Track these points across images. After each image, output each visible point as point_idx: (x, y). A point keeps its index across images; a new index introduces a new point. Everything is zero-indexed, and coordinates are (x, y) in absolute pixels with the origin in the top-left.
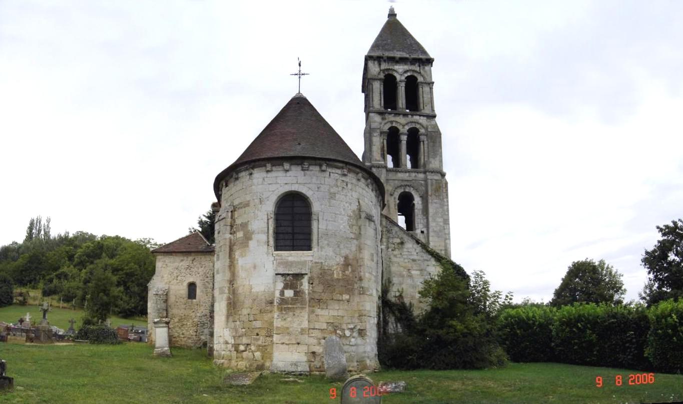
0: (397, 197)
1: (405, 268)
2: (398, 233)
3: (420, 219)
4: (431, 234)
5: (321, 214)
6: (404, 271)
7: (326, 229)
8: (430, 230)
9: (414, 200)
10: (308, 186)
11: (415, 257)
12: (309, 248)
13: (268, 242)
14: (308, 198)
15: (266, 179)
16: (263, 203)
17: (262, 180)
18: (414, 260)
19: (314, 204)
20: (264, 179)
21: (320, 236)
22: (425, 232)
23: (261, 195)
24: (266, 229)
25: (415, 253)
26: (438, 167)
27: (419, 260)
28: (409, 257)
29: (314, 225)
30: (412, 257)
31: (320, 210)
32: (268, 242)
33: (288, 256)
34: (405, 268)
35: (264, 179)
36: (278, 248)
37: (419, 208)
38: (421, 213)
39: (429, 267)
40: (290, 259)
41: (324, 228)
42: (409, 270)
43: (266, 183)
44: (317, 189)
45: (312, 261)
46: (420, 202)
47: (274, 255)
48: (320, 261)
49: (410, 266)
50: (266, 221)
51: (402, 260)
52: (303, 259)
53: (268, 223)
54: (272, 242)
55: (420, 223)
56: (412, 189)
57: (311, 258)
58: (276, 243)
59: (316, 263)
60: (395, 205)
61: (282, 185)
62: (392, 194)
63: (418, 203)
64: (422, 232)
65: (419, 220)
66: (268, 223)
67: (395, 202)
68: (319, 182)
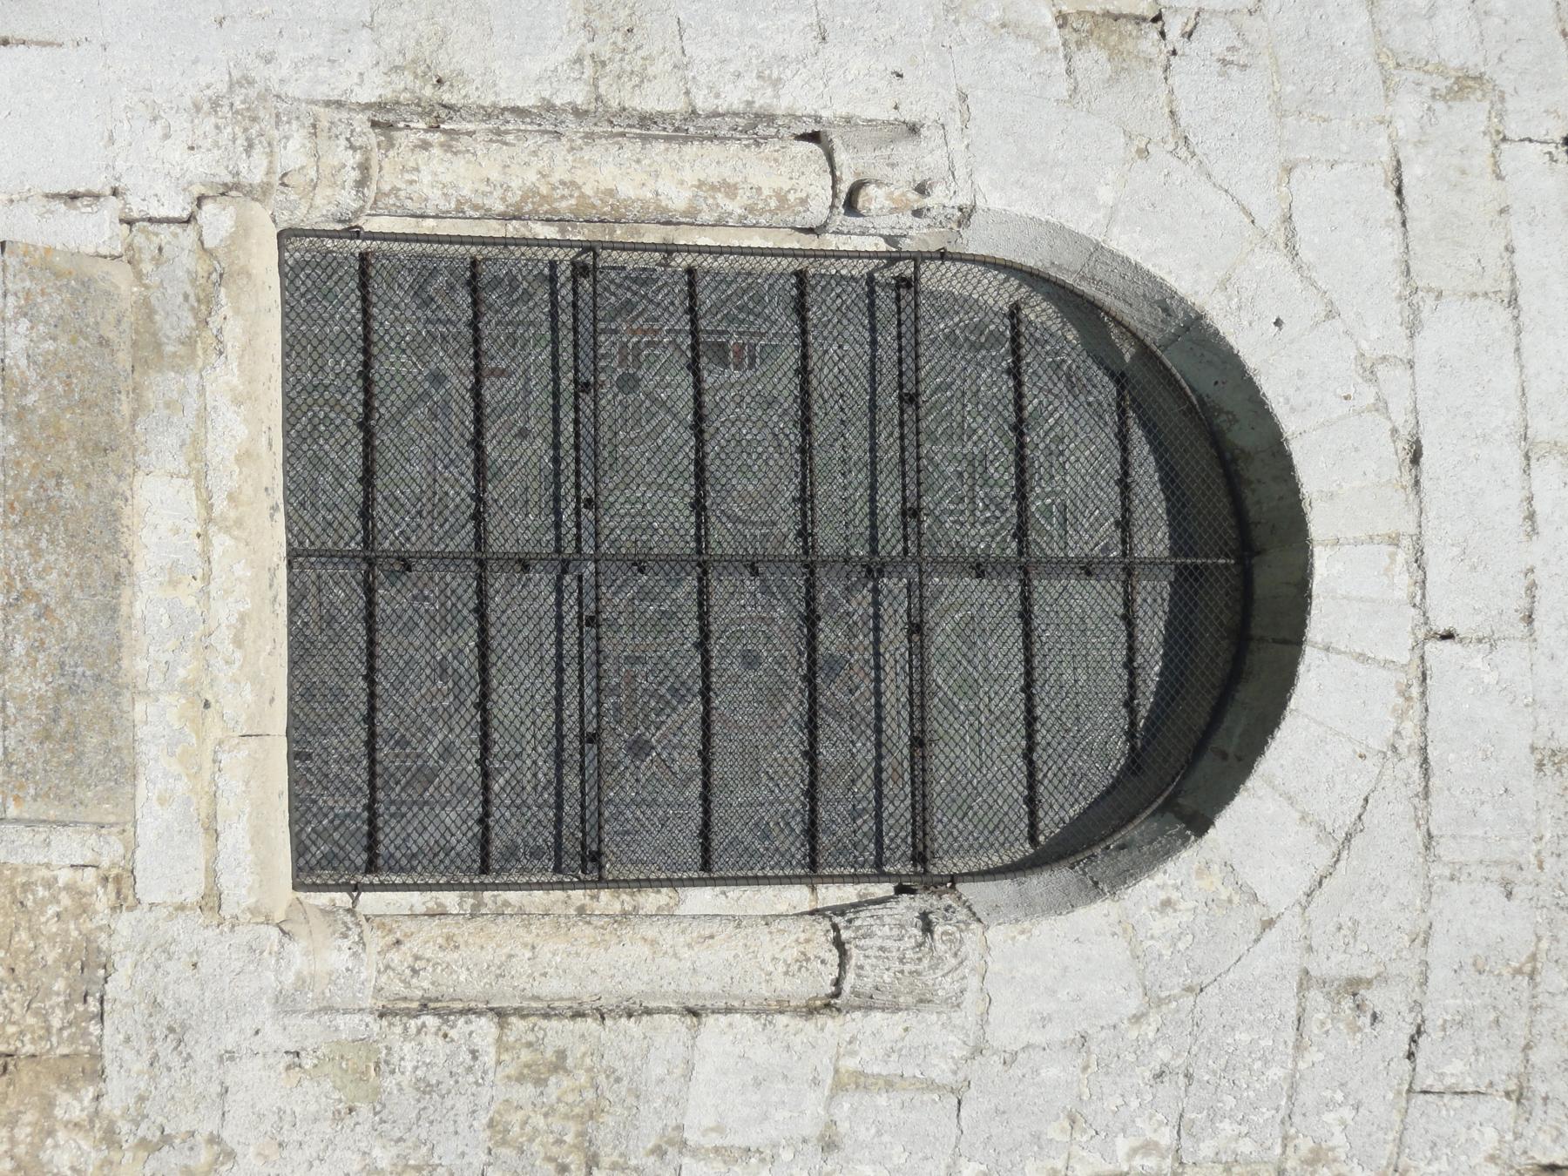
5: (938, 1041)
7: (673, 1144)
10: (1392, 819)
12: (351, 834)
13: (438, 116)
14: (1200, 824)
15: (1472, 116)
16: (1093, 61)
17: (1457, 50)
19: (1097, 914)
20: (1465, 84)
21: (559, 1033)
23: (1214, 38)
24: (661, 98)
29: (747, 933)
31: (1003, 1034)
32: (438, 116)
33: (199, 472)
35: (1465, 84)
36: (348, 296)
40: (158, 509)
41: (698, 1123)
43: (1408, 109)
44: (1334, 964)
45: (121, 884)
47: (218, 220)
48: (112, 1038)
50: (799, 97)
52: (155, 720)
53: (755, 126)
54: (446, 190)
57: (166, 875)
58: (424, 270)
59: (91, 964)
61: (1394, 380)
66: (755, 126)
68: (1443, 1004)
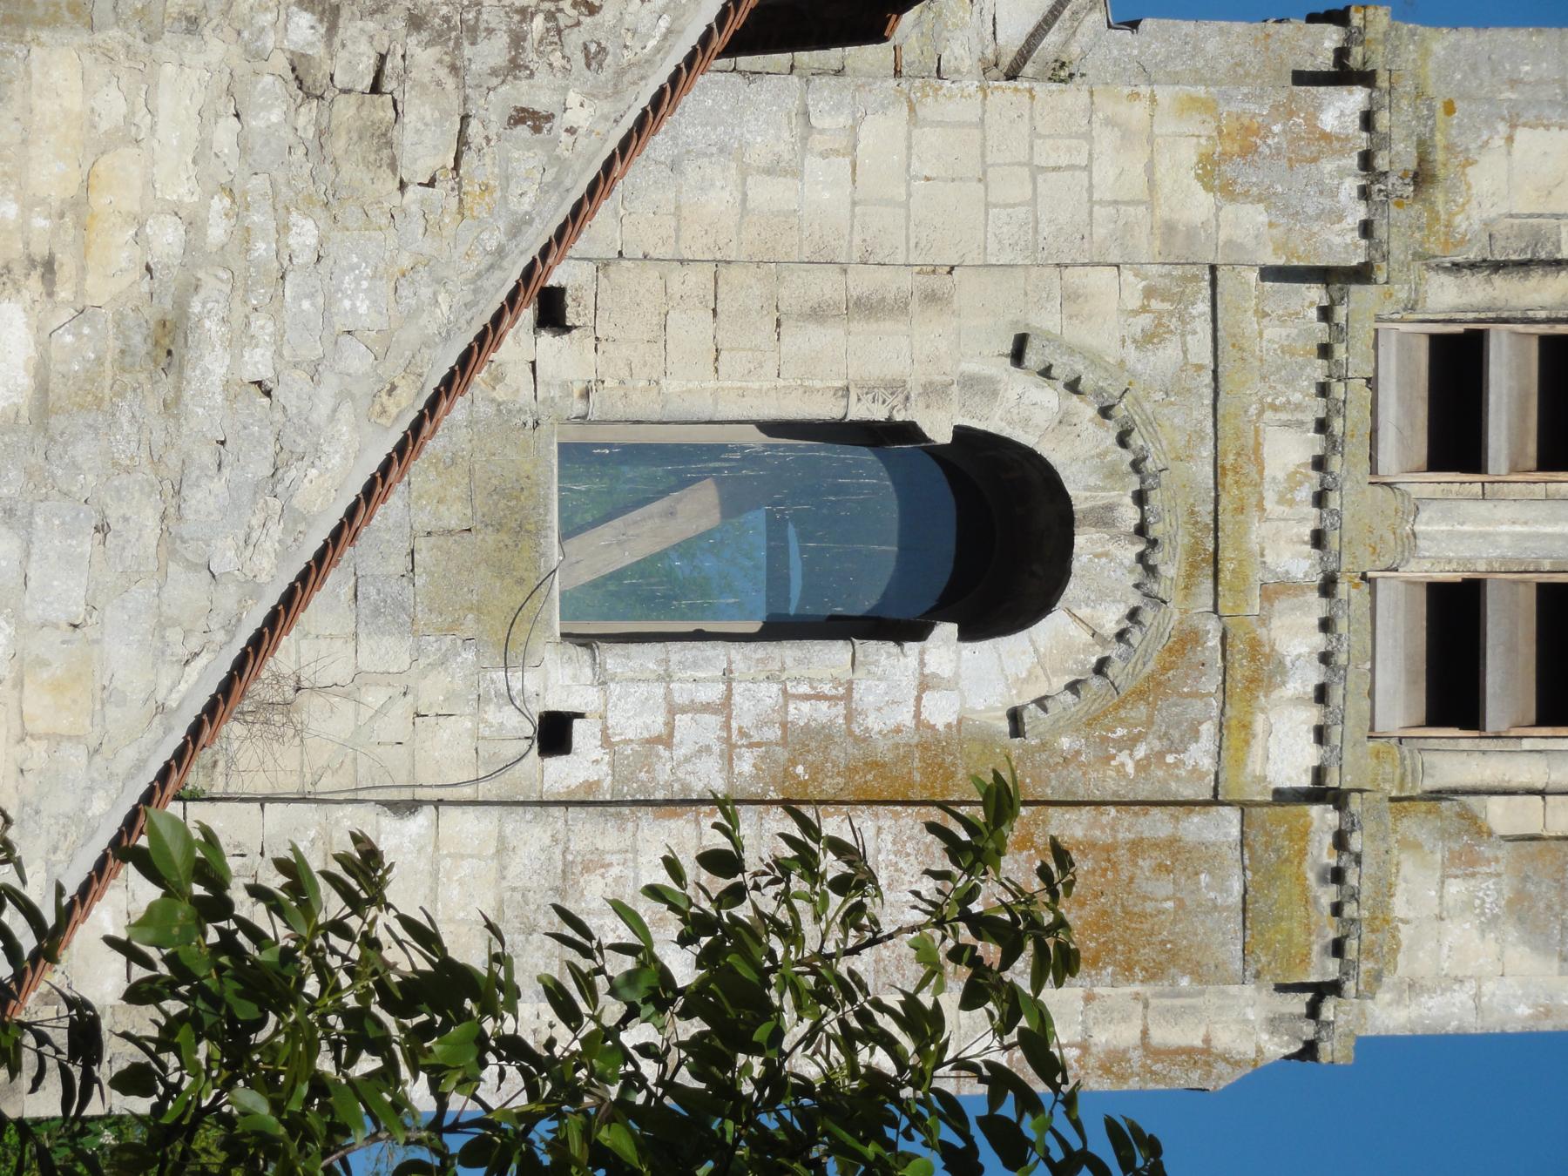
0: (993, 422)
1: (77, 210)
2: (525, 155)
3: (724, 707)
4: (533, 838)
6: (27, 207)
8: (587, 832)
9: (967, 634)
11: (212, 365)
18: (168, 343)
22: (560, 774)
25: (258, 363)
26: (1403, 966)
27: (172, 407)
28: (214, 284)
30: (210, 316)
34: (77, 210)
37: (868, 693)
38: (801, 712)
39: (87, 544)
42: (49, 267)
46: (941, 711)
49: (100, 290)
51: (181, 189)
55: (673, 710)
56: (1111, 618)
60: (895, 387)
62: (1032, 358)
63: (925, 684)
64: (554, 733)
65: (714, 693)
67: (934, 392)
